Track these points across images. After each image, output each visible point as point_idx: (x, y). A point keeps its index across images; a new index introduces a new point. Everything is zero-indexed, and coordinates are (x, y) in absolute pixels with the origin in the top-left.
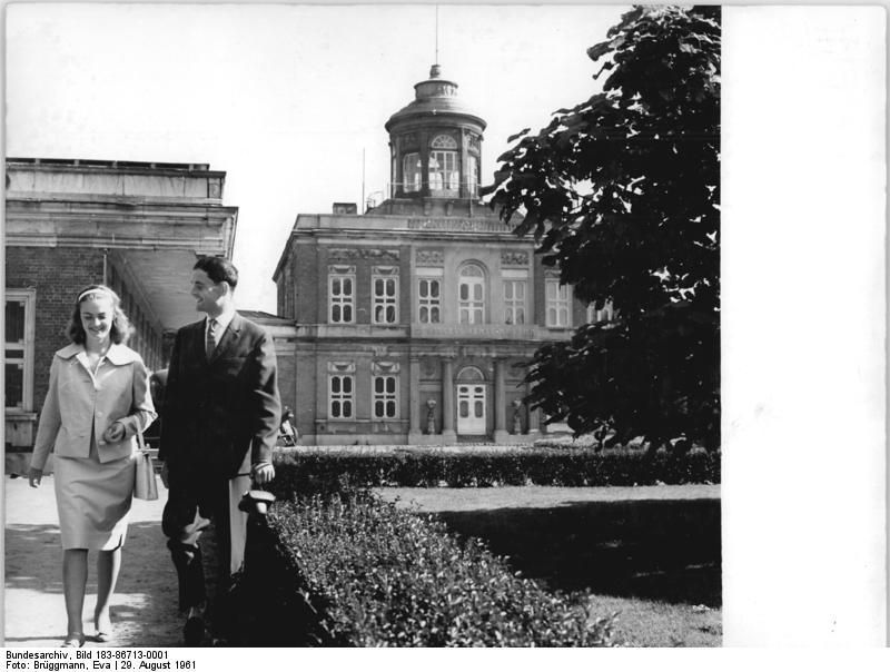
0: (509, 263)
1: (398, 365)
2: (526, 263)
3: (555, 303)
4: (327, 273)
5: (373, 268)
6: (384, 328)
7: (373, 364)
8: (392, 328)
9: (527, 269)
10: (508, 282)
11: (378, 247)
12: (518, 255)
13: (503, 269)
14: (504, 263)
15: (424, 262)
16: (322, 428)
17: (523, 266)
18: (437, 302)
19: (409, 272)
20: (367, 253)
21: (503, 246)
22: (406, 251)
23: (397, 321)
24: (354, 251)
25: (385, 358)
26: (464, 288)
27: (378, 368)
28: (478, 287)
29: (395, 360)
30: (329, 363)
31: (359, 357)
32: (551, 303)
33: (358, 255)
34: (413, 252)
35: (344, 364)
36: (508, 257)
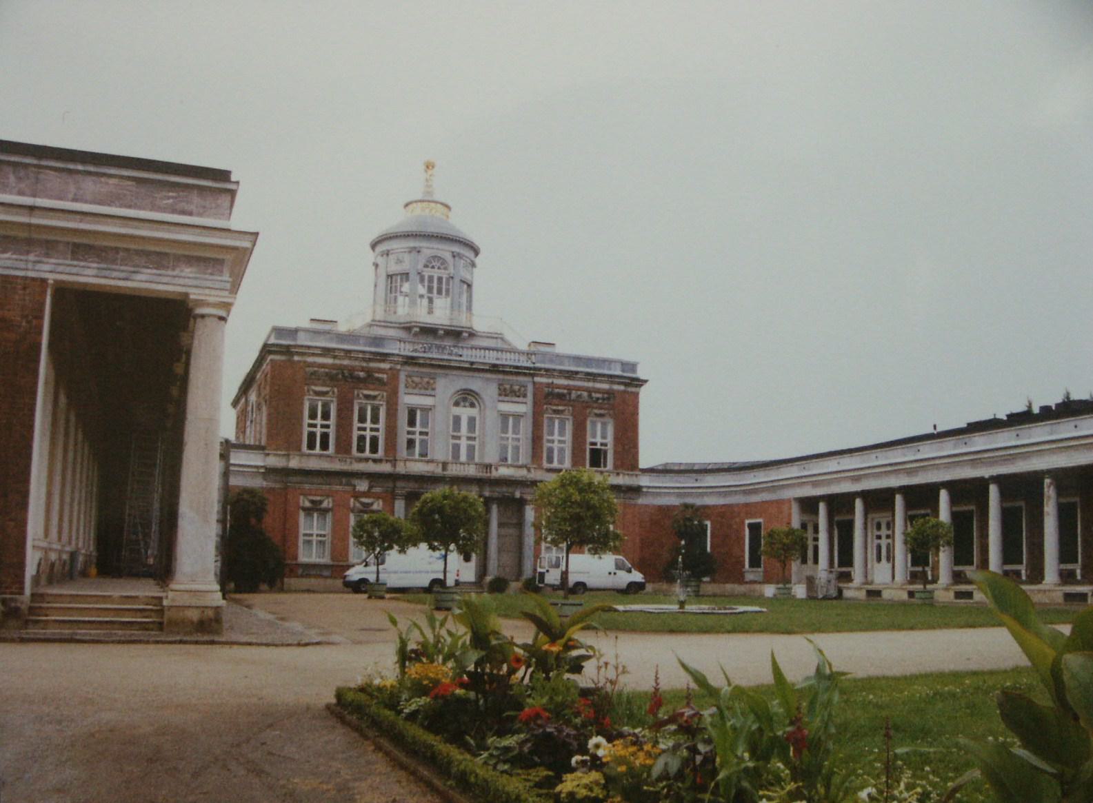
0: (506, 395)
1: (381, 502)
2: (525, 396)
3: (508, 439)
4: (303, 395)
5: (356, 392)
6: (367, 460)
7: (352, 500)
8: (375, 461)
9: (526, 403)
10: (505, 417)
11: (363, 369)
12: (516, 388)
13: (499, 401)
14: (500, 395)
15: (414, 386)
16: (291, 571)
17: (521, 399)
18: (426, 434)
19: (397, 398)
20: (352, 376)
21: (501, 376)
22: (394, 375)
23: (381, 453)
24: (335, 372)
25: (365, 494)
26: (457, 420)
27: (358, 505)
28: (472, 421)
29: (377, 497)
30: (302, 497)
31: (337, 492)
32: (549, 441)
33: (340, 376)
34: (402, 376)
35: (318, 498)
36: (505, 389)
